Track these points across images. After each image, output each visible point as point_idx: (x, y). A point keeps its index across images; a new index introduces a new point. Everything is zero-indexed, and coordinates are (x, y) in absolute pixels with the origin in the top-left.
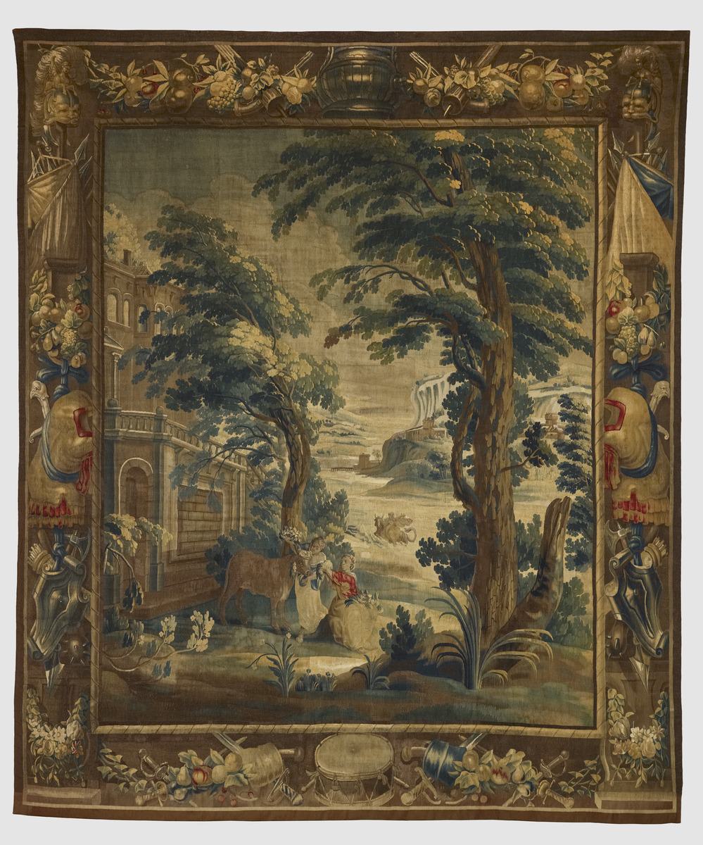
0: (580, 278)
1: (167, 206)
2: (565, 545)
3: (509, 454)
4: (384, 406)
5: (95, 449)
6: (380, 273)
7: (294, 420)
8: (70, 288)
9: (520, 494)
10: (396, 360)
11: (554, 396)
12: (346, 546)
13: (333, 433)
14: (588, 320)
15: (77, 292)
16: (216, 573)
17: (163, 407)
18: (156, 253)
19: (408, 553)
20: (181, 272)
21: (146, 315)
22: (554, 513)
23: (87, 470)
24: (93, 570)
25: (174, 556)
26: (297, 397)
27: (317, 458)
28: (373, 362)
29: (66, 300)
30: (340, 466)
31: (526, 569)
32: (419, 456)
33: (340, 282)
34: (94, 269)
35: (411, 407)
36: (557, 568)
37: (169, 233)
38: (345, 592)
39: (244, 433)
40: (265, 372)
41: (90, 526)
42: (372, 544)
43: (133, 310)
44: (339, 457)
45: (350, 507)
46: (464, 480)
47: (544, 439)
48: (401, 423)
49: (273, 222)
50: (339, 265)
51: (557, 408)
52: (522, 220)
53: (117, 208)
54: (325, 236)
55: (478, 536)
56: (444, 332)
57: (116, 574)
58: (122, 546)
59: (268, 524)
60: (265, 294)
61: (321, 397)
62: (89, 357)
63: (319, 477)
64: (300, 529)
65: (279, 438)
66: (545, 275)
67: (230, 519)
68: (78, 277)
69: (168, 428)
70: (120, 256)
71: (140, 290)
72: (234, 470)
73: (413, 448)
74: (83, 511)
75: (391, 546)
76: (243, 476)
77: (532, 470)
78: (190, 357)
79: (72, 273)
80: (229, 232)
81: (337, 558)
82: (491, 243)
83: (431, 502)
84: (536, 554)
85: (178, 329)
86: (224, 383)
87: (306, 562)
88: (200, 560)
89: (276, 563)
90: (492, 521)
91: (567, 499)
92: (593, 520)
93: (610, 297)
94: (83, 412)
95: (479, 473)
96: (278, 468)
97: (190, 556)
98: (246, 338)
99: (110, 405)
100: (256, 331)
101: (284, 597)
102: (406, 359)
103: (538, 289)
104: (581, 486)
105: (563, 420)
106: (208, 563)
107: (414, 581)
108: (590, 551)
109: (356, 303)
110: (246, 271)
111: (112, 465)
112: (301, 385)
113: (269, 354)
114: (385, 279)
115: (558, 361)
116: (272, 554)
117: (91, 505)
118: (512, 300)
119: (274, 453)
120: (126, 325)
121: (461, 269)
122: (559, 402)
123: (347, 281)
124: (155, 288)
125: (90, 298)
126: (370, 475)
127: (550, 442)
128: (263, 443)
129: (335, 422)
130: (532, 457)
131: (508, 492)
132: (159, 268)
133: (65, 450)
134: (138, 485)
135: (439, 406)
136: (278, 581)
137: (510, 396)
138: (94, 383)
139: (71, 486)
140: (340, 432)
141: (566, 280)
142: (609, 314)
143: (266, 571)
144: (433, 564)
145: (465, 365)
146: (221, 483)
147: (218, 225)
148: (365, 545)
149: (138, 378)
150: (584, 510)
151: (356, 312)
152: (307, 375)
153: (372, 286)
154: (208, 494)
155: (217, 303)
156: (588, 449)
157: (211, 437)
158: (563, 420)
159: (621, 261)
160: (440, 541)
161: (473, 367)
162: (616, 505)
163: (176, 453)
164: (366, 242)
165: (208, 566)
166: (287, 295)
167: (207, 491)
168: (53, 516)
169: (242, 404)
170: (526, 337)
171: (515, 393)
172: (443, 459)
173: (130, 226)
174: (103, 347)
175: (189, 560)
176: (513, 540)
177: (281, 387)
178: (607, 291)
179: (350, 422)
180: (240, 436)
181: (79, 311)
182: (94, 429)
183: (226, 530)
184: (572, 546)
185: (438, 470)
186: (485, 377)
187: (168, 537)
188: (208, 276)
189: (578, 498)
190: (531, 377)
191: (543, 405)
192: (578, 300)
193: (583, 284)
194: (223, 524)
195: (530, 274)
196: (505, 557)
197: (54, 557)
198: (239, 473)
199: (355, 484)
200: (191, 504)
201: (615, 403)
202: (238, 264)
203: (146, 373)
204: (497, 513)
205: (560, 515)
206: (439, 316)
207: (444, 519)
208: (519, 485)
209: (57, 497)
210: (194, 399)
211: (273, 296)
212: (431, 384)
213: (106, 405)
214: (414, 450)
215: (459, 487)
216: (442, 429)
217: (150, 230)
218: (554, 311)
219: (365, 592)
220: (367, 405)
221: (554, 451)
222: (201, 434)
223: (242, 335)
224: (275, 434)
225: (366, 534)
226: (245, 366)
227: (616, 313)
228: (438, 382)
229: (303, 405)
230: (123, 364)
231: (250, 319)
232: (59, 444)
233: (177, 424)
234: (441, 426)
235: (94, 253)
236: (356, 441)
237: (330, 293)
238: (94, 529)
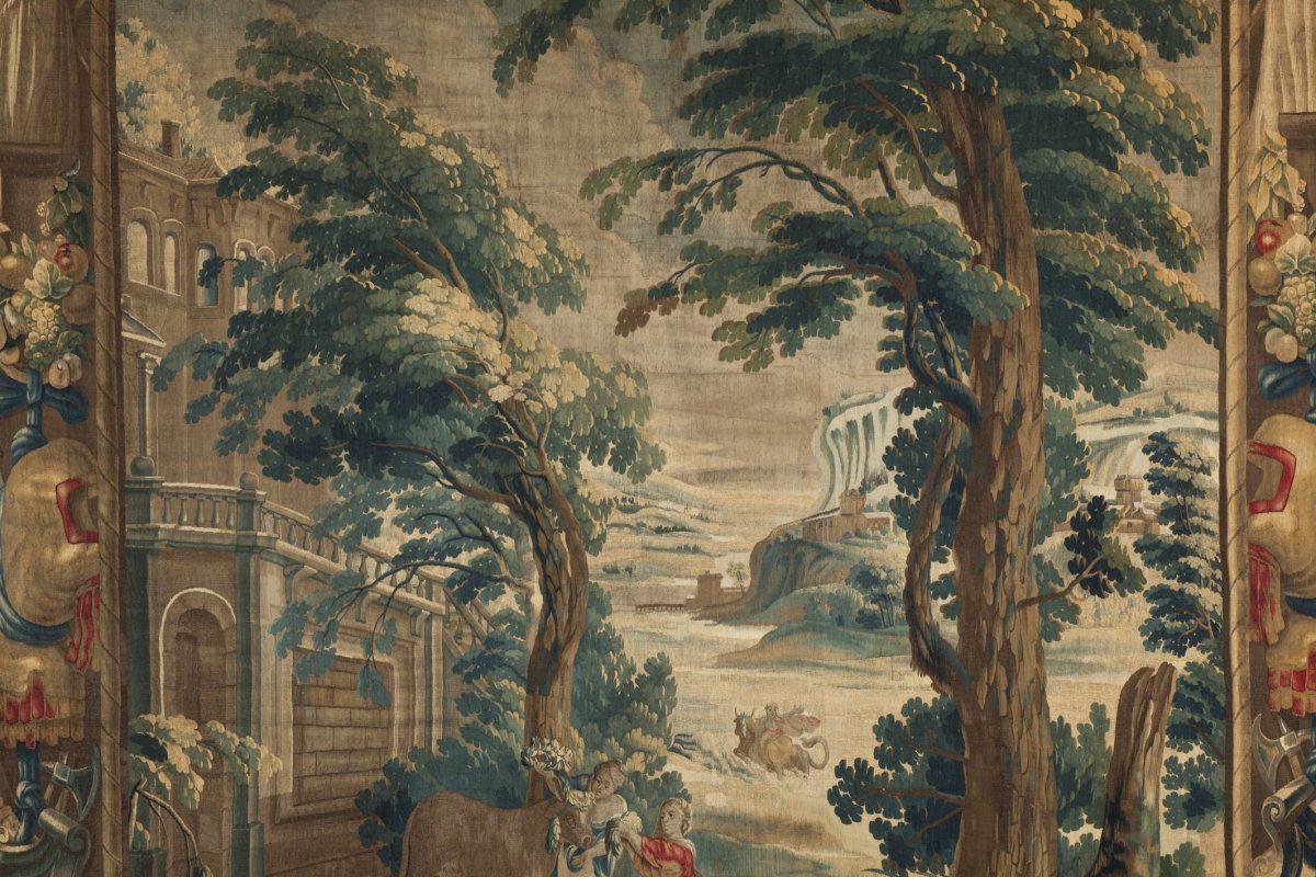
0: (1189, 171)
1: (260, 21)
2: (1164, 772)
3: (1034, 568)
4: (753, 465)
5: (106, 571)
6: (738, 165)
7: (550, 500)
8: (42, 209)
9: (1059, 658)
10: (779, 360)
11: (1133, 437)
12: (671, 780)
13: (639, 528)
14: (1208, 266)
15: (60, 219)
16: (381, 844)
17: (256, 473)
18: (234, 127)
19: (810, 794)
20: (290, 171)
21: (213, 267)
22: (1137, 700)
23: (88, 616)
24: (106, 840)
25: (287, 808)
26: (555, 447)
27: (602, 583)
28: (726, 366)
29: (36, 237)
30: (656, 601)
31: (1076, 825)
32: (831, 577)
33: (649, 187)
34: (97, 164)
35: (813, 467)
36: (1145, 824)
37: (263, 83)
39: (438, 530)
40: (484, 392)
41: (98, 742)
43: (185, 257)
44: (656, 581)
45: (679, 693)
46: (934, 628)
47: (1112, 535)
48: (792, 503)
49: (497, 53)
50: (647, 150)
51: (1141, 465)
52: (1056, 43)
53: (145, 27)
54: (613, 82)
55: (967, 755)
56: (885, 295)
57: (157, 849)
58: (169, 785)
59: (495, 733)
60: (480, 217)
61: (611, 446)
62: (88, 362)
63: (608, 626)
64: (567, 743)
65: (517, 539)
66: (1112, 165)
67: (409, 723)
68: (62, 185)
69: (268, 520)
70: (154, 135)
71: (200, 213)
72: (417, 613)
73: (818, 558)
74: (82, 709)
75: (771, 777)
76: (437, 627)
77: (1087, 603)
78: (315, 361)
79: (49, 174)
80: (399, 78)
82: (989, 94)
83: (861, 680)
84: (1098, 793)
85: (286, 297)
86: (388, 418)
87: (583, 816)
88: (347, 815)
89: (514, 819)
90: (998, 719)
91: (1167, 668)
92: (1225, 714)
93: (1258, 213)
94: (76, 487)
95: (968, 612)
96: (516, 607)
97: (323, 807)
98: (440, 315)
99: (136, 471)
100: (463, 299)
102: (798, 360)
103: (1096, 197)
104: (1197, 638)
105: (1154, 490)
106: (362, 822)
107: (823, 855)
108: (1220, 785)
109: (685, 232)
110: (437, 165)
111: (145, 606)
112: (566, 419)
113: (492, 350)
114: (750, 179)
115: (1141, 359)
116: (507, 801)
117: (98, 697)
118: (1038, 222)
119: (505, 572)
120: (170, 290)
121: (925, 151)
122: (1146, 451)
123: (666, 185)
124: (234, 206)
125: (88, 232)
126: (722, 619)
127: (1127, 541)
128: (481, 551)
129: (641, 502)
130: (1086, 574)
131: (1033, 654)
132: (243, 162)
133: (39, 573)
134: (203, 650)
135: (877, 464)
136: (521, 859)
137: (1036, 439)
138: (100, 423)
139: (52, 652)
140: (654, 524)
141: (1157, 175)
142: (1256, 250)
143: (493, 838)
144: (868, 818)
145: (934, 369)
146: (390, 642)
147: (372, 64)
148: (714, 777)
149: (199, 409)
150: (1205, 693)
151: (687, 253)
152: (577, 398)
153: (721, 195)
154: (359, 668)
155: (374, 237)
156: (1212, 556)
157: (365, 540)
158: (1154, 490)
159: (1281, 129)
160: (882, 766)
161: (952, 374)
162: (1277, 681)
163: (286, 576)
164: (706, 98)
165: (361, 827)
166: (531, 219)
167: (358, 661)
168: (11, 723)
169: (432, 464)
170: (1070, 305)
171: (1048, 433)
172: (887, 582)
173: (176, 70)
174: (120, 339)
175: (320, 816)
176: (1045, 763)
177: (520, 425)
178: (1251, 199)
179: (677, 501)
180: (429, 537)
181: (65, 261)
182: (101, 524)
183: (402, 748)
184: (1177, 774)
185: (876, 607)
186: (979, 397)
187: (273, 765)
188: (351, 177)
189: (1191, 666)
190: (1082, 395)
191: (1110, 457)
192: (1186, 221)
193: (1196, 183)
194: (396, 733)
195: (1078, 163)
196: (1028, 800)
197: (18, 813)
198: (428, 620)
199: (690, 641)
200: (322, 691)
201: (1271, 451)
202: (419, 149)
203: (217, 400)
204: (1009, 702)
205: (1152, 704)
206: (872, 260)
207: (891, 717)
208: (1058, 638)
209: (21, 679)
210: (325, 455)
211: (498, 221)
212: (856, 414)
213: (128, 470)
214: (822, 563)
215: (924, 647)
216: (884, 515)
217: (221, 76)
218: (1131, 245)
220: (715, 463)
221: (1137, 560)
222: (342, 533)
223: (430, 309)
224: (509, 531)
225: (717, 754)
226: (439, 379)
227: (1272, 247)
228: (874, 408)
229: (571, 463)
230: (164, 376)
231: (448, 272)
232: (25, 559)
233: (289, 511)
234: (881, 507)
235: (97, 130)
236: (691, 543)
237: (626, 211)
238: (105, 749)
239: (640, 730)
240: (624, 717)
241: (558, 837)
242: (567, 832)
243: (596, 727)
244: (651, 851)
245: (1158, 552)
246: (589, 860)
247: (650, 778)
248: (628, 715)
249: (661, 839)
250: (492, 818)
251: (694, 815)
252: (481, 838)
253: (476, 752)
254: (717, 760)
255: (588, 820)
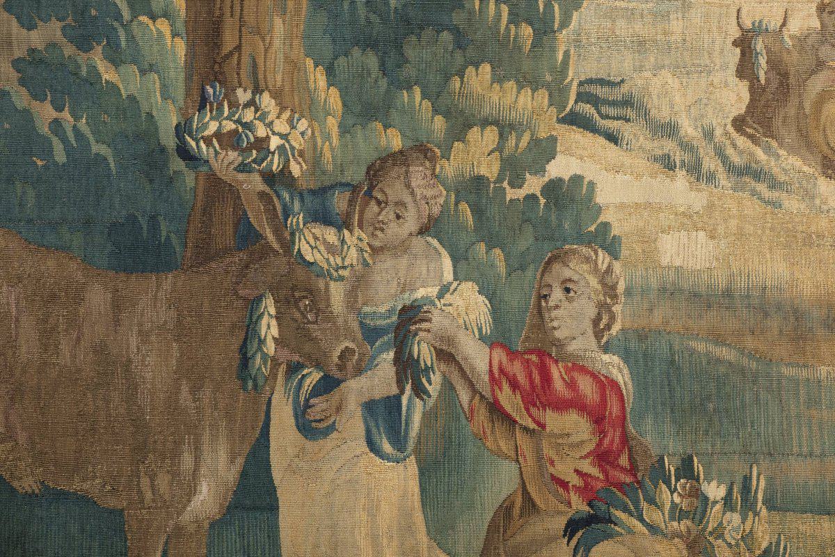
38: (564, 469)
42: (723, 178)
59: (108, 74)
64: (297, 102)
81: (517, 266)
87: (337, 293)
89: (155, 299)
101: (206, 499)
116: (137, 251)
143: (100, 350)
148: (679, 190)
219: (686, 469)
225: (688, 129)
239: (486, 68)
240: (446, 36)
241: (270, 348)
242: (295, 334)
243: (372, 61)
244: (514, 385)
246: (353, 407)
247: (511, 194)
248: (456, 31)
249: (542, 354)
250: (98, 298)
251: (628, 292)
252: (65, 348)
253: (56, 125)
254: (686, 146)
255: (352, 295)
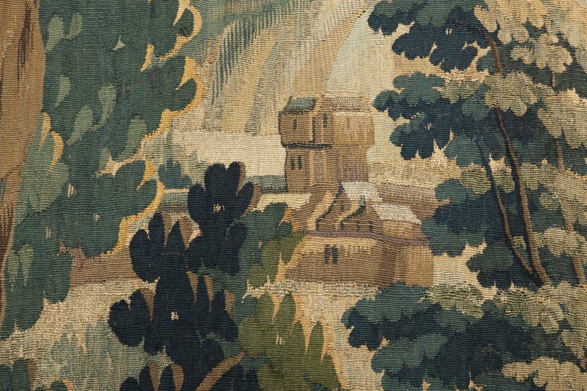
47: (274, 289)
105: (411, 144)
127: (324, 308)
158: (411, 144)
191: (263, 44)
245: (431, 344)
